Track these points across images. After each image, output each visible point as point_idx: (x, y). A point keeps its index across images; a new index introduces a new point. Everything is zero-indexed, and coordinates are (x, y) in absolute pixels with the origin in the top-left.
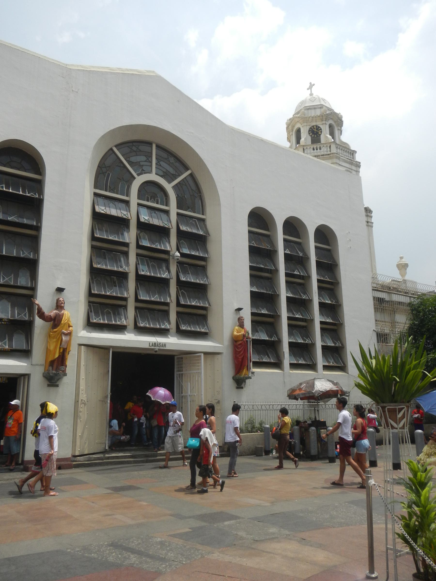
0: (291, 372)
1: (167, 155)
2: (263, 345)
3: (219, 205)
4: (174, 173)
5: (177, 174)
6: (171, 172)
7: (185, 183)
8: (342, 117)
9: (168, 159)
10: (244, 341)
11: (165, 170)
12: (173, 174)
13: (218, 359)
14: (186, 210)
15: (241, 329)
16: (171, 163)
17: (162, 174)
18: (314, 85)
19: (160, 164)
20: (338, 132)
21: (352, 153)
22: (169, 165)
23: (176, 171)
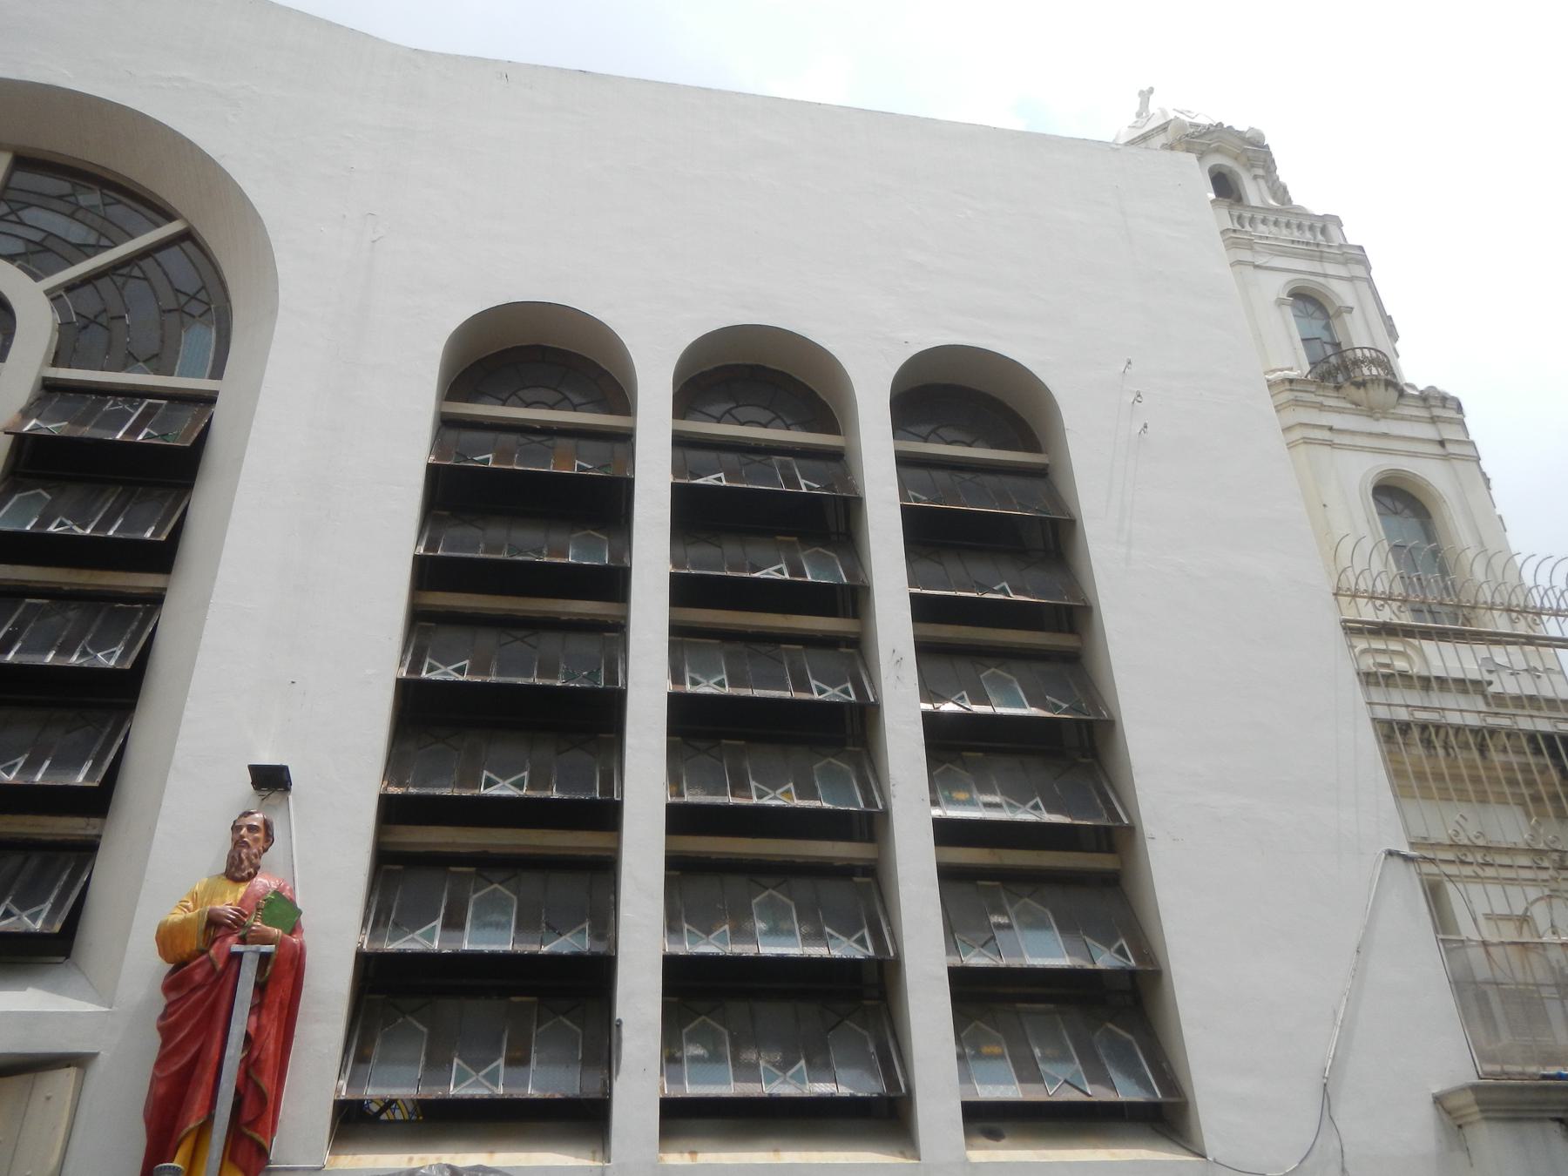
0: (676, 1159)
1: (74, 185)
2: (514, 999)
3: (274, 312)
4: (92, 239)
5: (104, 242)
6: (70, 239)
7: (143, 272)
8: (1262, 136)
9: (72, 199)
10: (210, 959)
11: (37, 236)
12: (78, 246)
13: (48, 1098)
14: (123, 368)
15: (227, 885)
16: (81, 207)
17: (18, 247)
18: (1151, 91)
19: (18, 217)
20: (1259, 186)
21: (1319, 225)
22: (71, 216)
23: (101, 234)
